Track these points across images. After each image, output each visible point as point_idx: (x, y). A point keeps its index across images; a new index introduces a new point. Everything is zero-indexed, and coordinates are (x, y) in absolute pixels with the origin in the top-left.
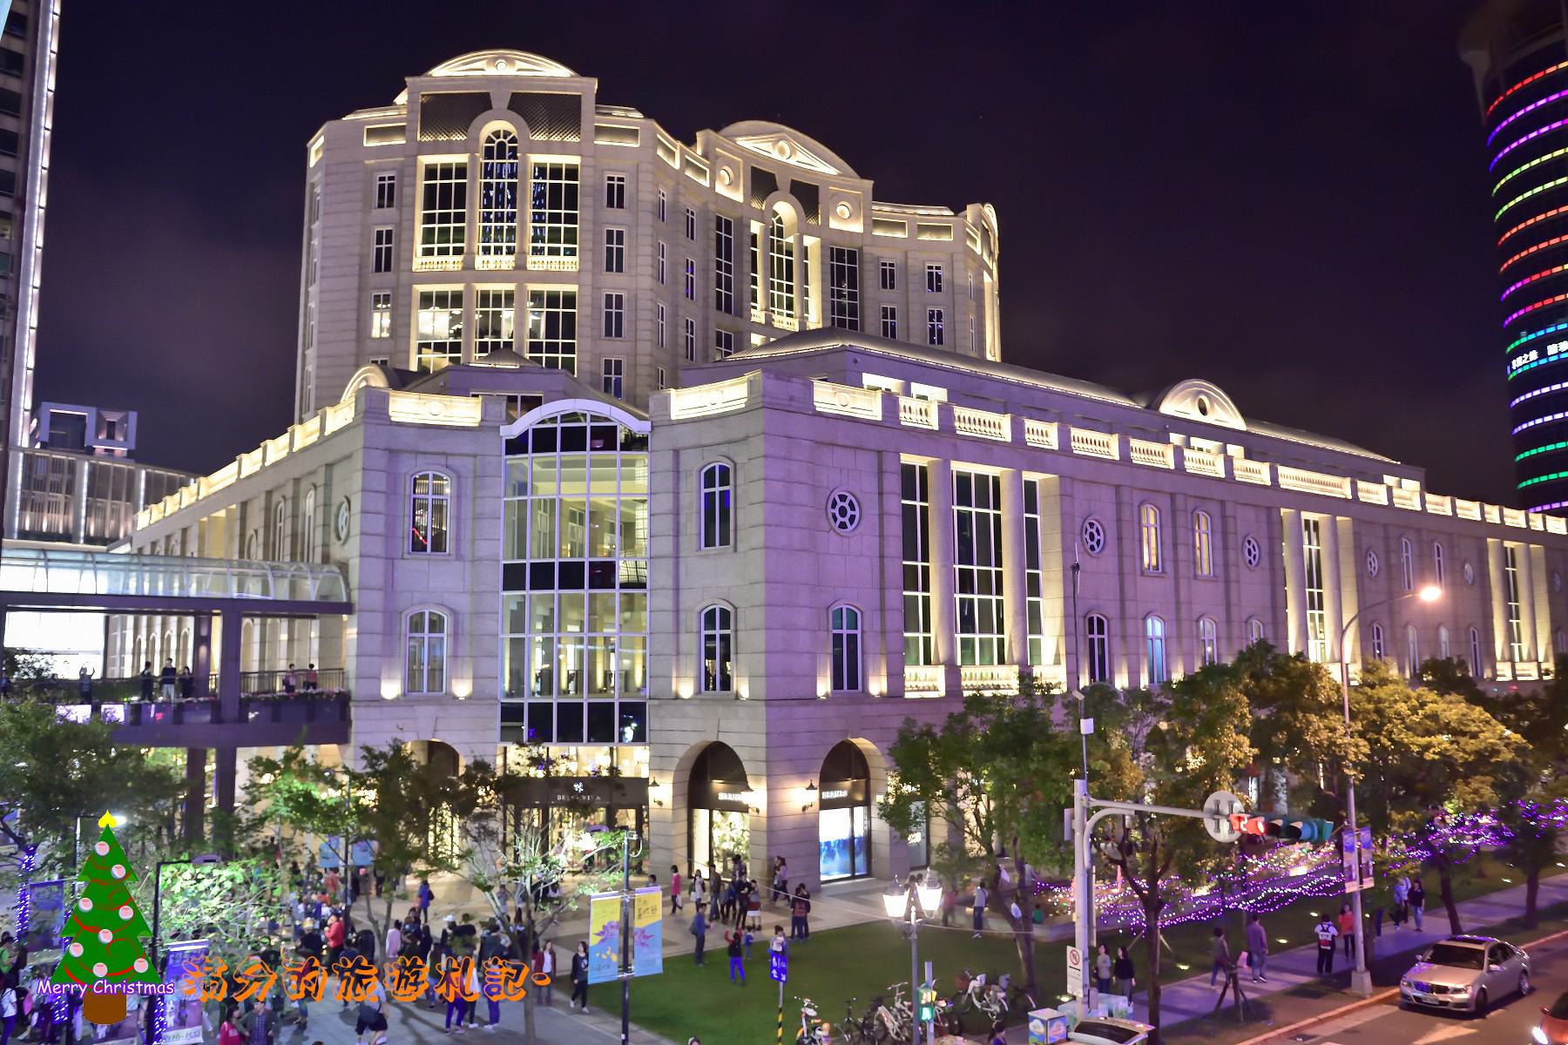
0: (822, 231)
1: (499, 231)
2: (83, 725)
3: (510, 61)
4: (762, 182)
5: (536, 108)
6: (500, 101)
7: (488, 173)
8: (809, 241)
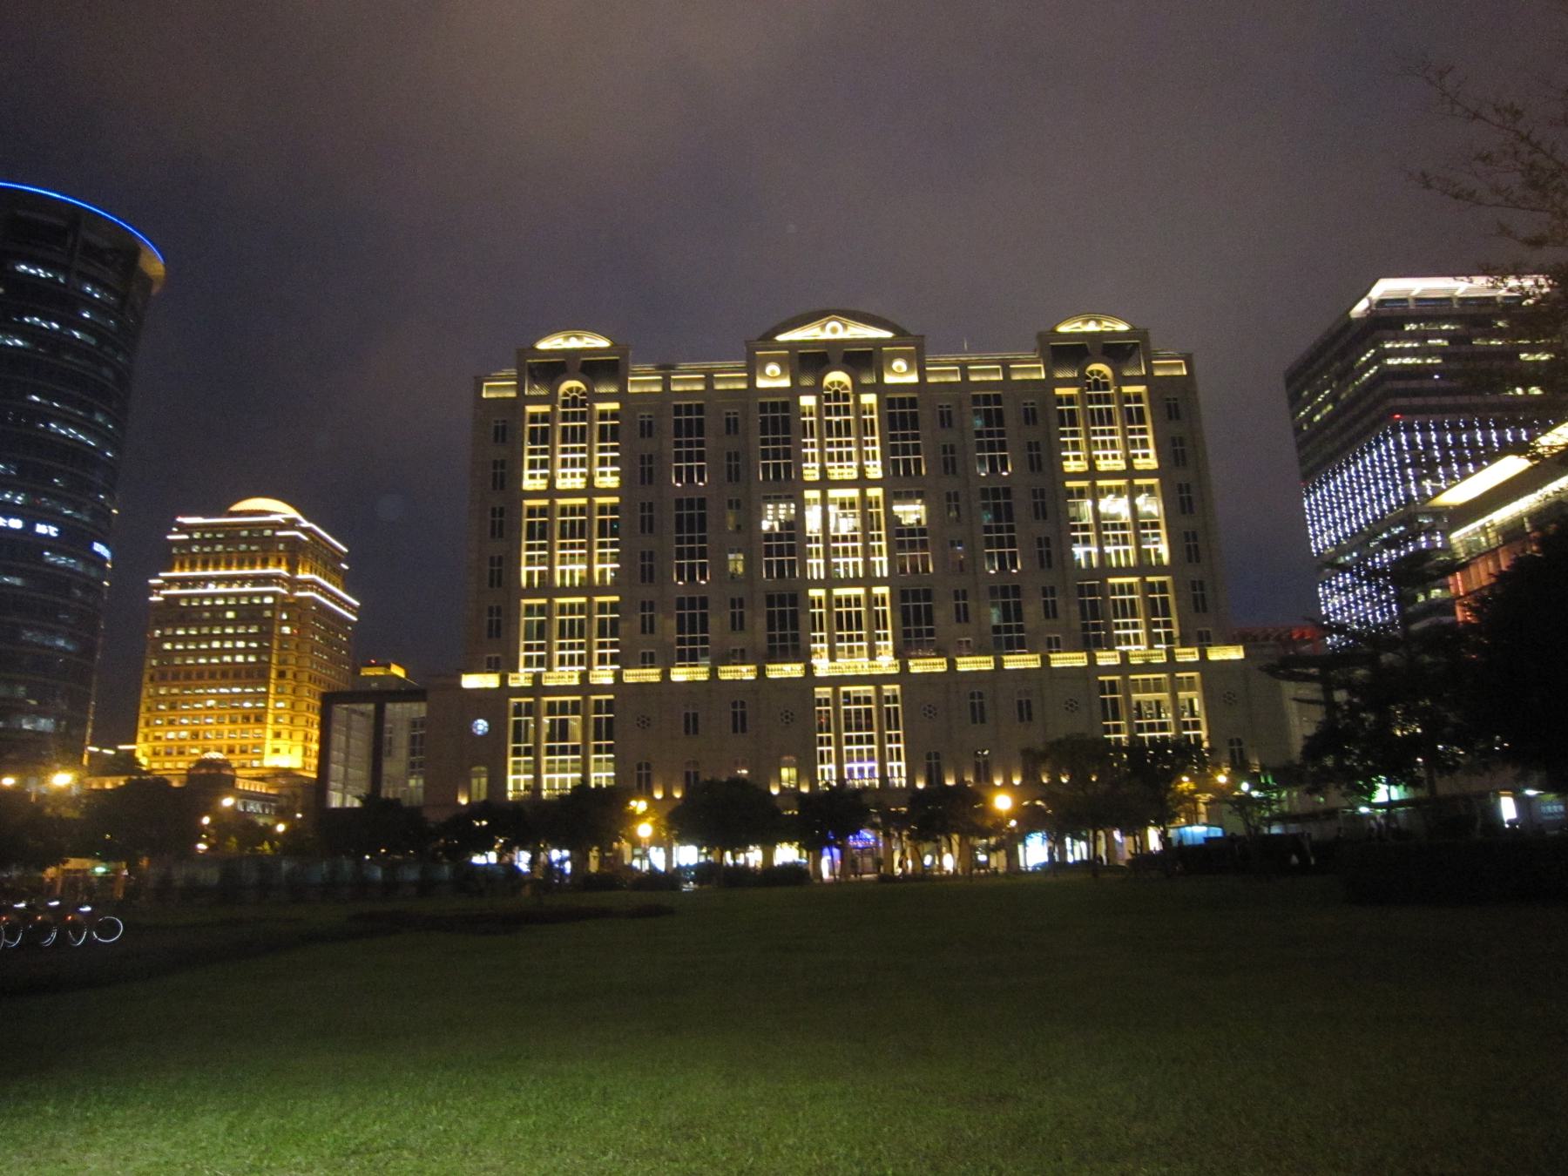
0: (879, 388)
3: (578, 337)
4: (812, 361)
5: (591, 367)
7: (565, 417)
8: (869, 399)
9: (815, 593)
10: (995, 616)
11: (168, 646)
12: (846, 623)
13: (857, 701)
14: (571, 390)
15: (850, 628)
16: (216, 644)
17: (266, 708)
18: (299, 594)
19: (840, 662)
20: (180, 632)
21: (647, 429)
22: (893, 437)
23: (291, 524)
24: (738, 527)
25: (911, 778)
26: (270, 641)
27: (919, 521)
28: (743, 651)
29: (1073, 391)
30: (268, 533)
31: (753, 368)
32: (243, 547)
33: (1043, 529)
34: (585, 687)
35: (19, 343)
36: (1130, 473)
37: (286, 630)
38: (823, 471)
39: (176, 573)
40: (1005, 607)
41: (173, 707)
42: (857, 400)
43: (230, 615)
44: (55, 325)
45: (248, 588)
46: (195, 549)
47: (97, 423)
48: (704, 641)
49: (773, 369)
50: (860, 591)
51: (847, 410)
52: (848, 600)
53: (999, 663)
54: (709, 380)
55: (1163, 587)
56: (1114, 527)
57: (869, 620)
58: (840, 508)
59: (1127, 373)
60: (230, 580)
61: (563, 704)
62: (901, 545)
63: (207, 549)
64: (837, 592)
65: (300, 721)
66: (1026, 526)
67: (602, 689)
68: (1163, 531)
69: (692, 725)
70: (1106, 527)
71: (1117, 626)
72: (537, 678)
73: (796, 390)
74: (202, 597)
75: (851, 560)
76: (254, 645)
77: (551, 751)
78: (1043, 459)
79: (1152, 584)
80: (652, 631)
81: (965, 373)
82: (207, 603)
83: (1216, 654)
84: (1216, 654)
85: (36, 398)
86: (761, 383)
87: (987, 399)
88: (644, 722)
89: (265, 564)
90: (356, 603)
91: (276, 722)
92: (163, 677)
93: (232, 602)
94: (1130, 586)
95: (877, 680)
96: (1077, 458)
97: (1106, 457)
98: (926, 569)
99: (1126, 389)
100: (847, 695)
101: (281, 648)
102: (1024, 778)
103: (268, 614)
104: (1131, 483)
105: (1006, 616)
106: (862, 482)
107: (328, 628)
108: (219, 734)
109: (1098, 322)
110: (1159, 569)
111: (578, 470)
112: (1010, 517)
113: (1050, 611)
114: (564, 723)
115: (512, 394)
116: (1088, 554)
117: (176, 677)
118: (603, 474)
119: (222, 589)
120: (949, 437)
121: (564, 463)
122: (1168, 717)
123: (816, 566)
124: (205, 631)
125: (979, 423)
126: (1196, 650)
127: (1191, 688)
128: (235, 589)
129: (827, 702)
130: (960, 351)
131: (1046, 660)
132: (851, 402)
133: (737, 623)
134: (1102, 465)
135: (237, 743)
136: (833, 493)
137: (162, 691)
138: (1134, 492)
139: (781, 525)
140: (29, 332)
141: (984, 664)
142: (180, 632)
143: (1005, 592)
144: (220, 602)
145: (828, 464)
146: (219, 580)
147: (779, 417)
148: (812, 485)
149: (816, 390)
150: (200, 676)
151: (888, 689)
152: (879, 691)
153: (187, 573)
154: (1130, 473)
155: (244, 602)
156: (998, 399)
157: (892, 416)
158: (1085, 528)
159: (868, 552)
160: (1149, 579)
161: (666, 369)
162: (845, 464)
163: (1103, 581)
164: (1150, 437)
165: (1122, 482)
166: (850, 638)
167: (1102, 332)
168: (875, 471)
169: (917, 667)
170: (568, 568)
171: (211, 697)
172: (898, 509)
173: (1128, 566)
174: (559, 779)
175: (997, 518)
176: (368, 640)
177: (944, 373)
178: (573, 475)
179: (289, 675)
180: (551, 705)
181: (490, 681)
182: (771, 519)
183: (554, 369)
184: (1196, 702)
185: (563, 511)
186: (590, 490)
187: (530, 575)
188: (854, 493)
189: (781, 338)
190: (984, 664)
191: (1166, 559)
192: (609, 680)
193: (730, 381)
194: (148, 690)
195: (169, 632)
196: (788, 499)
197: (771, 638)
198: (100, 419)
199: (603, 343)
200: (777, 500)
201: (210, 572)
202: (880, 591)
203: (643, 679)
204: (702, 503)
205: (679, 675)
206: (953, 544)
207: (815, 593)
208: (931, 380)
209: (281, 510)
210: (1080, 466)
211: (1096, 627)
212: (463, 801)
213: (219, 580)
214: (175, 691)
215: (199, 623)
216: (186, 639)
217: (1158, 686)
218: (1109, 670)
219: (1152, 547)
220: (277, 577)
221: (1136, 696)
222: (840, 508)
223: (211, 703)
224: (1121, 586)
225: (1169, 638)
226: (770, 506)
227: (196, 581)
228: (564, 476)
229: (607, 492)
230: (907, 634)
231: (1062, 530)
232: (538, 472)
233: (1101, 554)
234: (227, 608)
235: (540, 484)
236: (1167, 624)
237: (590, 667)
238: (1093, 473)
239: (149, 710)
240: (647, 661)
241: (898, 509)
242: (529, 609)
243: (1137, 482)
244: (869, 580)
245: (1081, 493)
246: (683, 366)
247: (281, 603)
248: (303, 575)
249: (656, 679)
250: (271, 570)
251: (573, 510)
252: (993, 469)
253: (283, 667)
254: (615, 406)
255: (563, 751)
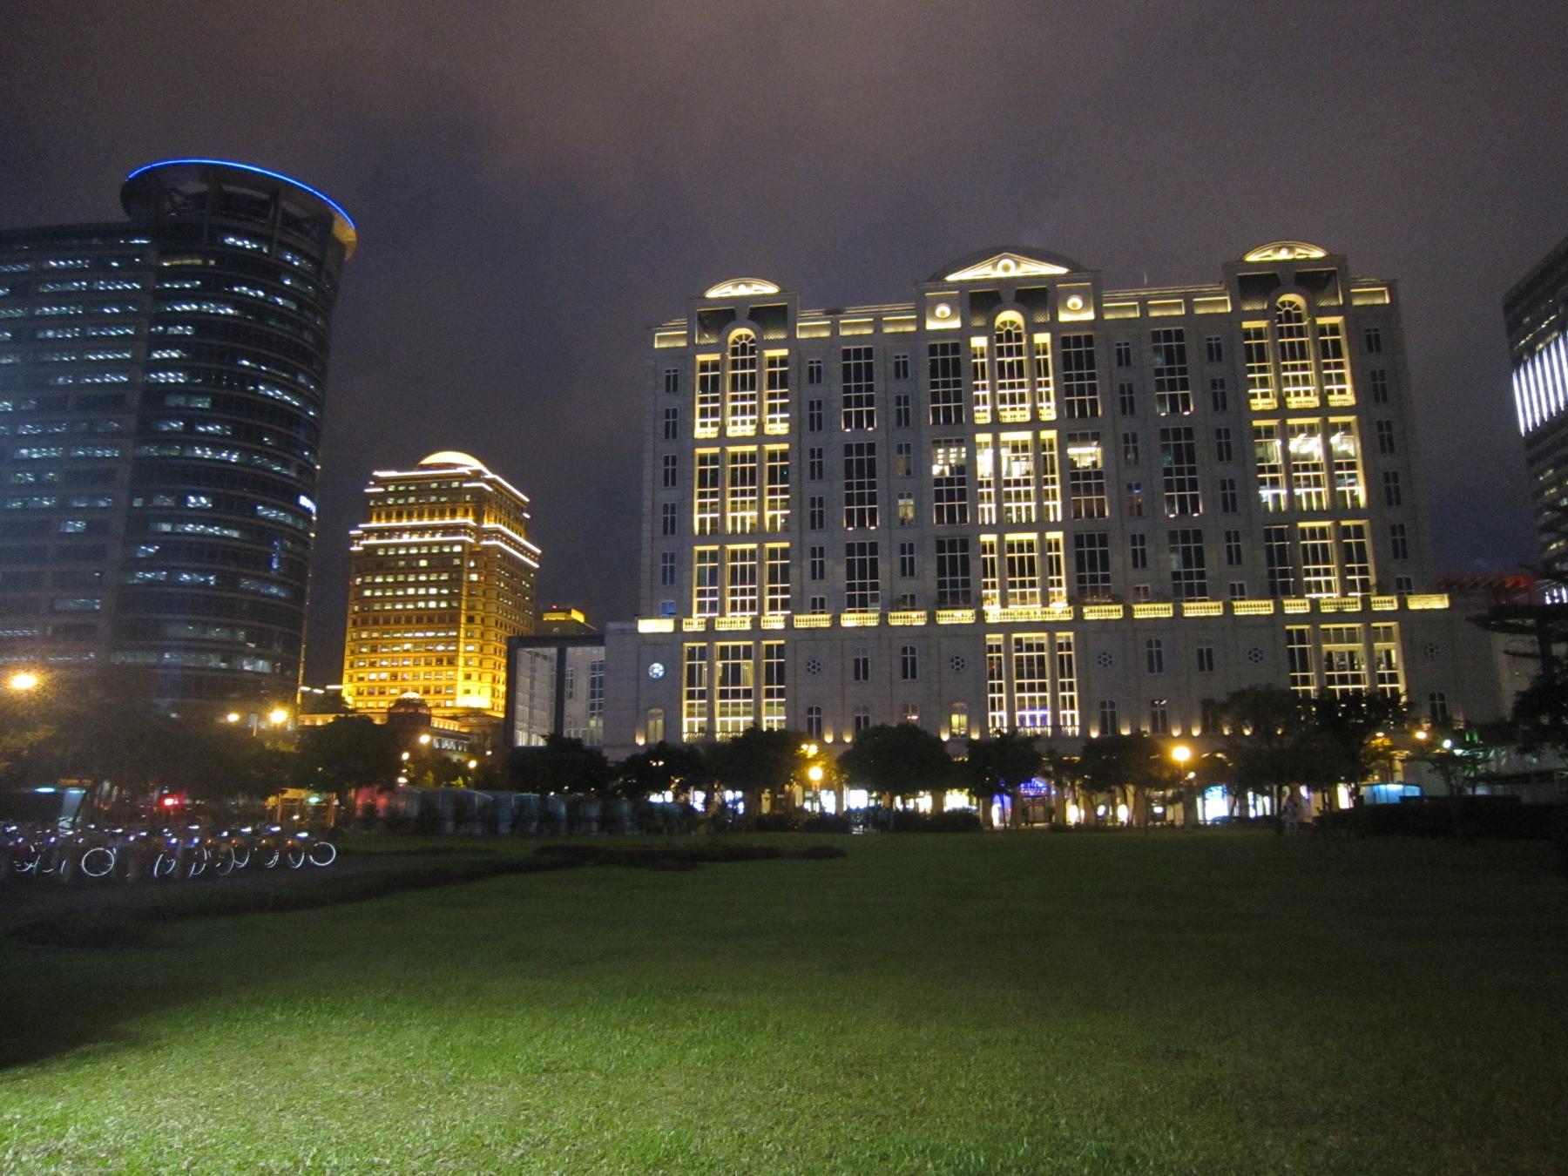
0: (1053, 326)
1: (744, 408)
2: (952, 788)
4: (983, 300)
5: (763, 315)
6: (743, 314)
7: (735, 365)
8: (1043, 338)
9: (988, 538)
10: (1175, 562)
11: (368, 593)
12: (1019, 568)
13: (1030, 647)
14: (740, 337)
15: (1022, 574)
16: (411, 591)
17: (457, 651)
18: (485, 543)
19: (1012, 608)
20: (379, 580)
21: (815, 375)
22: (1068, 378)
23: (477, 475)
24: (908, 472)
25: (1084, 728)
26: (460, 587)
27: (1095, 464)
28: (912, 597)
29: (1262, 324)
30: (456, 484)
31: (923, 309)
32: (433, 499)
33: (1223, 470)
34: (757, 631)
35: (230, 311)
36: (1324, 410)
37: (474, 577)
38: (995, 413)
39: (374, 524)
40: (1186, 552)
41: (374, 650)
42: (1030, 340)
43: (423, 563)
44: (261, 293)
45: (438, 538)
46: (390, 501)
47: (301, 385)
48: (875, 586)
49: (943, 309)
50: (1033, 536)
51: (1019, 351)
52: (1021, 545)
53: (1178, 611)
54: (878, 323)
55: (1359, 531)
56: (1306, 468)
57: (1042, 564)
58: (1011, 448)
59: (1323, 304)
60: (422, 530)
61: (736, 649)
62: (1076, 489)
63: (401, 501)
64: (1009, 537)
65: (488, 664)
66: (1208, 468)
67: (773, 634)
68: (1359, 472)
69: (861, 670)
70: (1296, 468)
71: (1308, 573)
72: (710, 623)
73: (967, 332)
74: (397, 546)
75: (1023, 505)
76: (445, 591)
77: (724, 695)
78: (1227, 398)
79: (1348, 528)
80: (822, 577)
81: (1145, 309)
82: (402, 552)
83: (1416, 603)
84: (1416, 603)
85: (246, 363)
86: (931, 325)
87: (1168, 334)
88: (814, 667)
89: (453, 514)
90: (538, 551)
91: (466, 665)
92: (365, 622)
93: (424, 551)
94: (1323, 530)
95: (1051, 627)
96: (1265, 396)
97: (1297, 394)
98: (1102, 514)
99: (1321, 321)
100: (1019, 641)
101: (470, 595)
102: (1205, 729)
103: (457, 562)
104: (1325, 420)
105: (1187, 562)
106: (1035, 424)
107: (512, 576)
108: (416, 677)
109: (1291, 249)
110: (1356, 512)
111: (748, 418)
112: (1191, 459)
113: (1234, 557)
114: (737, 668)
115: (683, 344)
116: (1276, 497)
117: (376, 622)
118: (773, 421)
119: (415, 538)
120: (1124, 375)
121: (734, 411)
122: (1363, 670)
123: (988, 510)
124: (401, 578)
125: (1159, 361)
126: (1394, 598)
127: (1388, 638)
128: (427, 538)
129: (998, 649)
130: (1138, 284)
131: (1229, 608)
132: (1024, 342)
133: (907, 569)
134: (1293, 403)
135: (432, 685)
136: (1006, 436)
137: (364, 635)
138: (1328, 431)
139: (951, 469)
140: (238, 301)
141: (1163, 611)
142: (379, 580)
143: (1185, 536)
144: (414, 551)
145: (1001, 407)
146: (413, 530)
147: (948, 359)
148: (984, 429)
149: (986, 330)
150: (397, 621)
151: (1062, 636)
152: (1052, 638)
153: (383, 524)
154: (1324, 410)
155: (435, 550)
156: (1179, 335)
157: (1066, 355)
158: (1273, 469)
159: (1042, 496)
160: (1344, 523)
161: (834, 312)
162: (1018, 406)
163: (1293, 524)
164: (1347, 372)
165: (1315, 420)
166: (1023, 585)
167: (1294, 260)
168: (1049, 412)
169: (1092, 614)
170: (739, 515)
171: (408, 640)
172: (1072, 451)
173: (1320, 509)
174: (731, 723)
175: (1178, 460)
176: (550, 587)
177: (1122, 309)
178: (744, 423)
179: (478, 620)
180: (724, 650)
181: (665, 626)
182: (941, 464)
183: (723, 316)
184: (1393, 653)
185: (734, 458)
186: (760, 437)
187: (702, 522)
188: (1026, 436)
189: (951, 278)
190: (1163, 611)
191: (1362, 500)
192: (781, 626)
193: (899, 323)
194: (351, 634)
195: (369, 579)
196: (960, 443)
197: (942, 584)
198: (302, 379)
199: (771, 289)
200: (948, 444)
201: (405, 523)
202: (1052, 536)
203: (813, 625)
204: (871, 448)
205: (850, 620)
206: (1130, 487)
207: (988, 538)
208: (1108, 317)
209: (467, 463)
210: (1270, 404)
211: (1284, 574)
212: (641, 741)
213: (413, 530)
214: (375, 635)
215: (395, 571)
216: (384, 586)
217: (1352, 636)
218: (1297, 618)
219: (1347, 489)
220: (465, 526)
221: (1326, 647)
222: (1011, 448)
223: (408, 646)
224: (1312, 530)
225: (1365, 586)
226: (940, 451)
227: (392, 531)
228: (735, 423)
229: (777, 439)
230: (1081, 580)
231: (1254, 471)
232: (709, 420)
233: (1291, 495)
234: (419, 556)
235: (711, 432)
236: (1363, 571)
237: (762, 613)
238: (1282, 411)
239: (353, 652)
240: (817, 606)
241: (1072, 451)
242: (702, 555)
243: (1332, 420)
244: (1042, 525)
245: (1269, 432)
246: (851, 310)
247: (470, 552)
248: (488, 524)
249: (827, 624)
250: (459, 520)
251: (744, 457)
252: (1174, 408)
253: (472, 613)
254: (784, 352)
255: (736, 694)
